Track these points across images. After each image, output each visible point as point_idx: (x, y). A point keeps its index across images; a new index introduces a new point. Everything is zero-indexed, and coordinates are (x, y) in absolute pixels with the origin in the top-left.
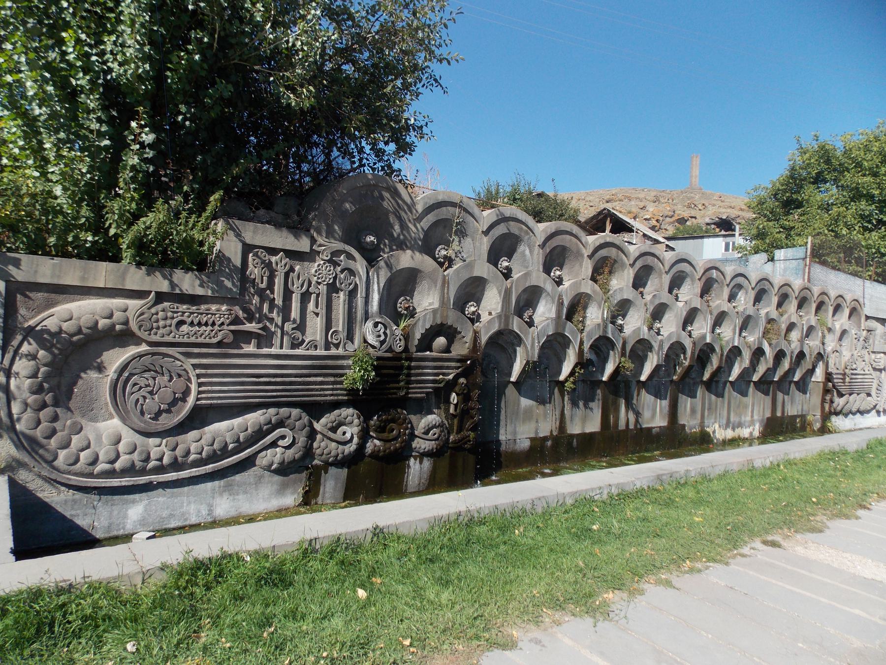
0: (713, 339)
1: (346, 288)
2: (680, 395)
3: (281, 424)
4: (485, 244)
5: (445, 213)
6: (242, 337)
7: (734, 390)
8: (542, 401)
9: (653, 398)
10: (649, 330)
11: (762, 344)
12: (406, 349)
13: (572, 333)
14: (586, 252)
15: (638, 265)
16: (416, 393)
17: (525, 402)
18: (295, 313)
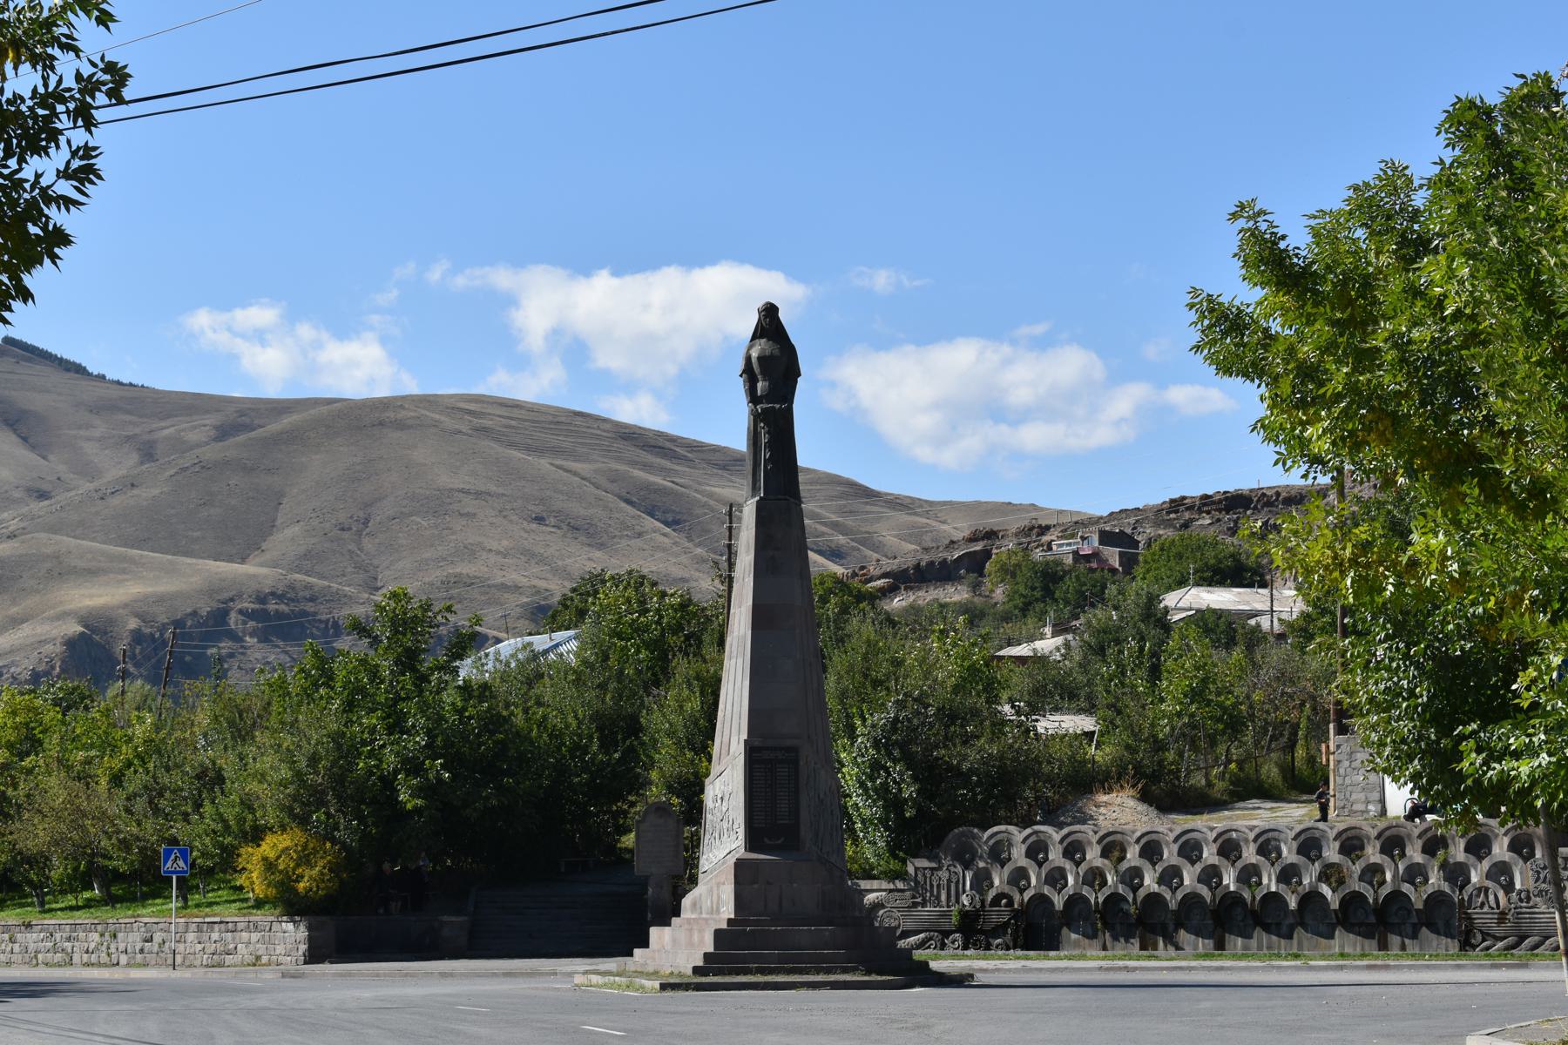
0: (1238, 888)
1: (954, 881)
2: (1227, 935)
3: (931, 939)
4: (1023, 848)
5: (999, 837)
6: (915, 905)
7: (1307, 931)
8: (1085, 935)
9: (1193, 937)
10: (1159, 886)
11: (1317, 887)
12: (983, 905)
13: (1088, 893)
14: (1095, 839)
15: (1143, 841)
16: (987, 928)
17: (1074, 936)
18: (935, 893)
